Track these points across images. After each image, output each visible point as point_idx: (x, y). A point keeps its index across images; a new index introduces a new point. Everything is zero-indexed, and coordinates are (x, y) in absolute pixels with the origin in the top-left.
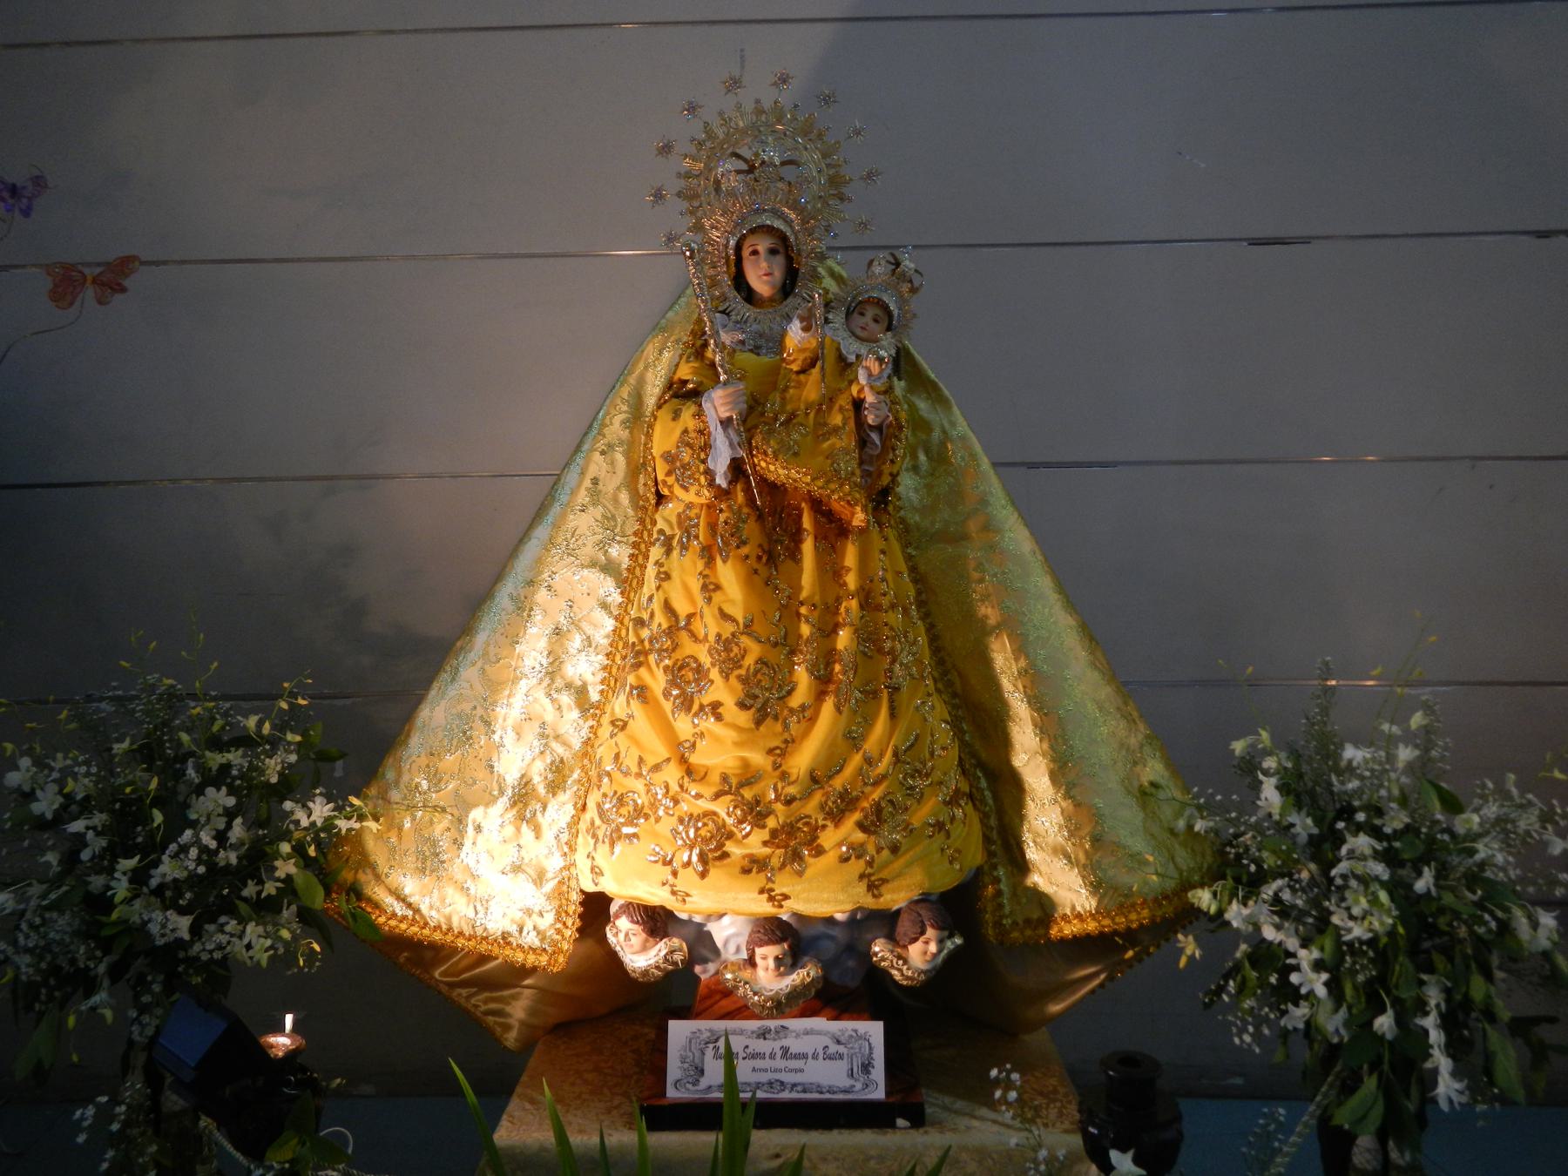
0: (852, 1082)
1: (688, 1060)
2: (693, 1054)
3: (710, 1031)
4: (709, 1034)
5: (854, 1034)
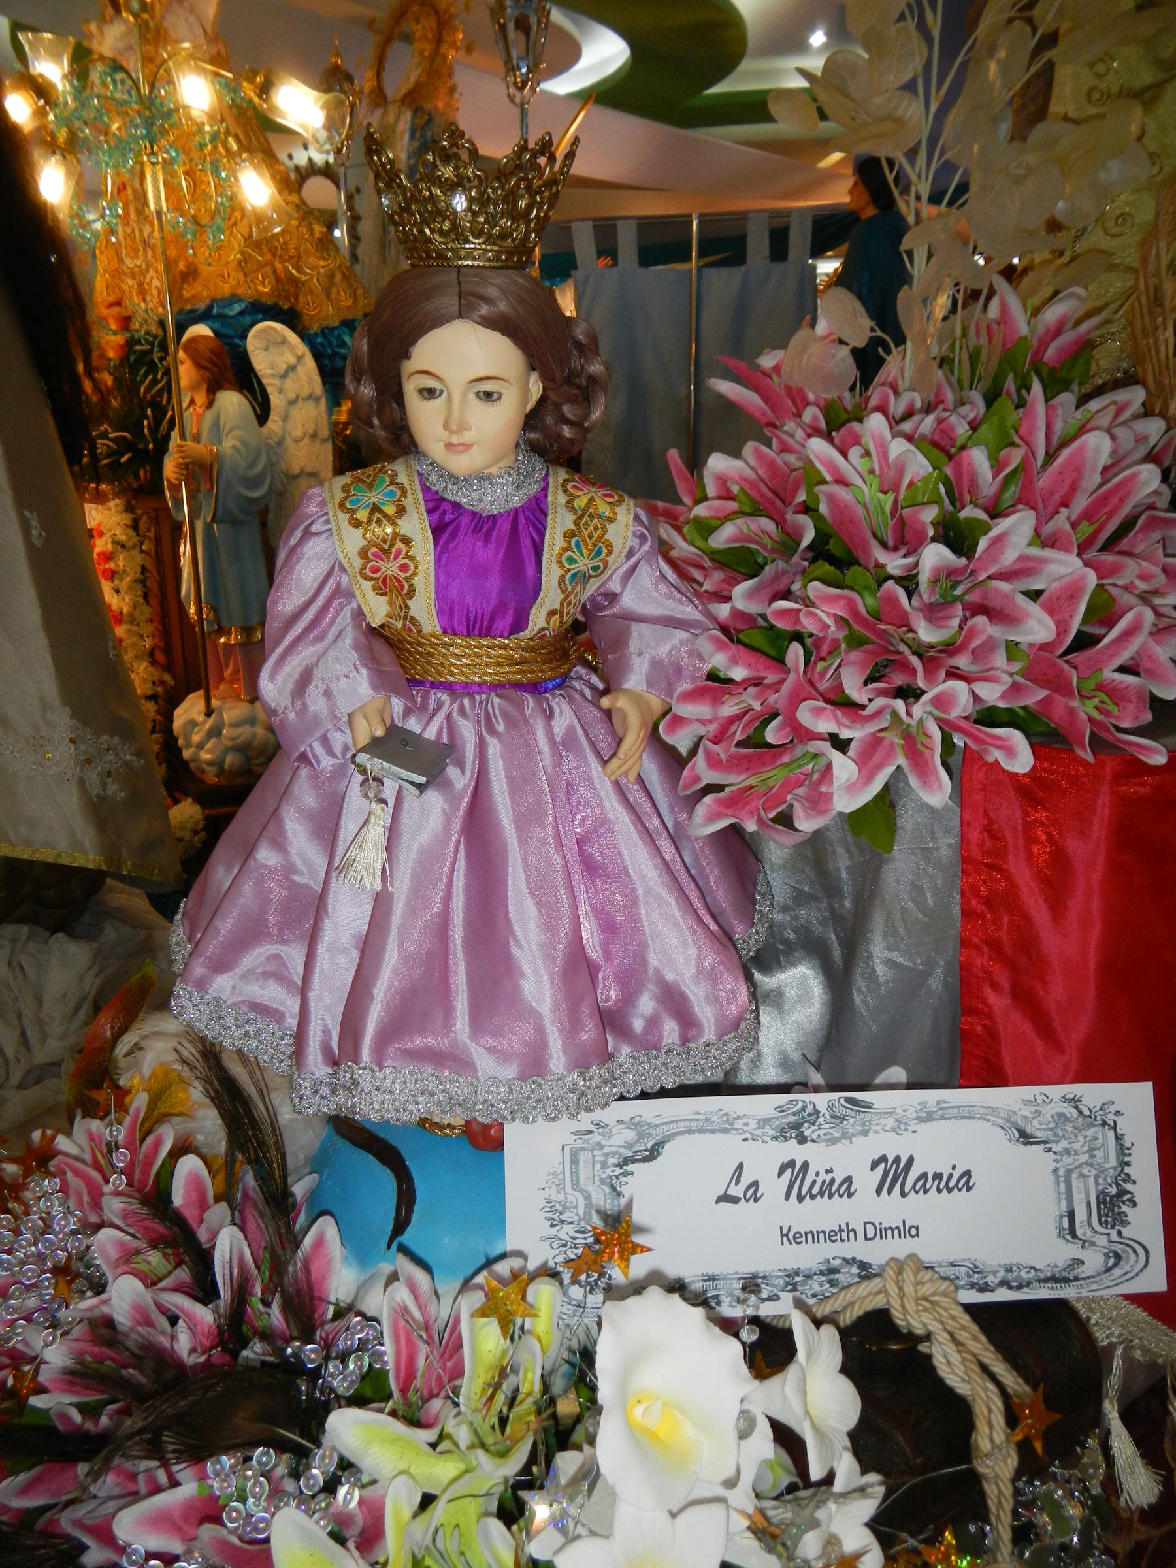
0: (1072, 1251)
1: (563, 1217)
3: (634, 1124)
4: (630, 1135)
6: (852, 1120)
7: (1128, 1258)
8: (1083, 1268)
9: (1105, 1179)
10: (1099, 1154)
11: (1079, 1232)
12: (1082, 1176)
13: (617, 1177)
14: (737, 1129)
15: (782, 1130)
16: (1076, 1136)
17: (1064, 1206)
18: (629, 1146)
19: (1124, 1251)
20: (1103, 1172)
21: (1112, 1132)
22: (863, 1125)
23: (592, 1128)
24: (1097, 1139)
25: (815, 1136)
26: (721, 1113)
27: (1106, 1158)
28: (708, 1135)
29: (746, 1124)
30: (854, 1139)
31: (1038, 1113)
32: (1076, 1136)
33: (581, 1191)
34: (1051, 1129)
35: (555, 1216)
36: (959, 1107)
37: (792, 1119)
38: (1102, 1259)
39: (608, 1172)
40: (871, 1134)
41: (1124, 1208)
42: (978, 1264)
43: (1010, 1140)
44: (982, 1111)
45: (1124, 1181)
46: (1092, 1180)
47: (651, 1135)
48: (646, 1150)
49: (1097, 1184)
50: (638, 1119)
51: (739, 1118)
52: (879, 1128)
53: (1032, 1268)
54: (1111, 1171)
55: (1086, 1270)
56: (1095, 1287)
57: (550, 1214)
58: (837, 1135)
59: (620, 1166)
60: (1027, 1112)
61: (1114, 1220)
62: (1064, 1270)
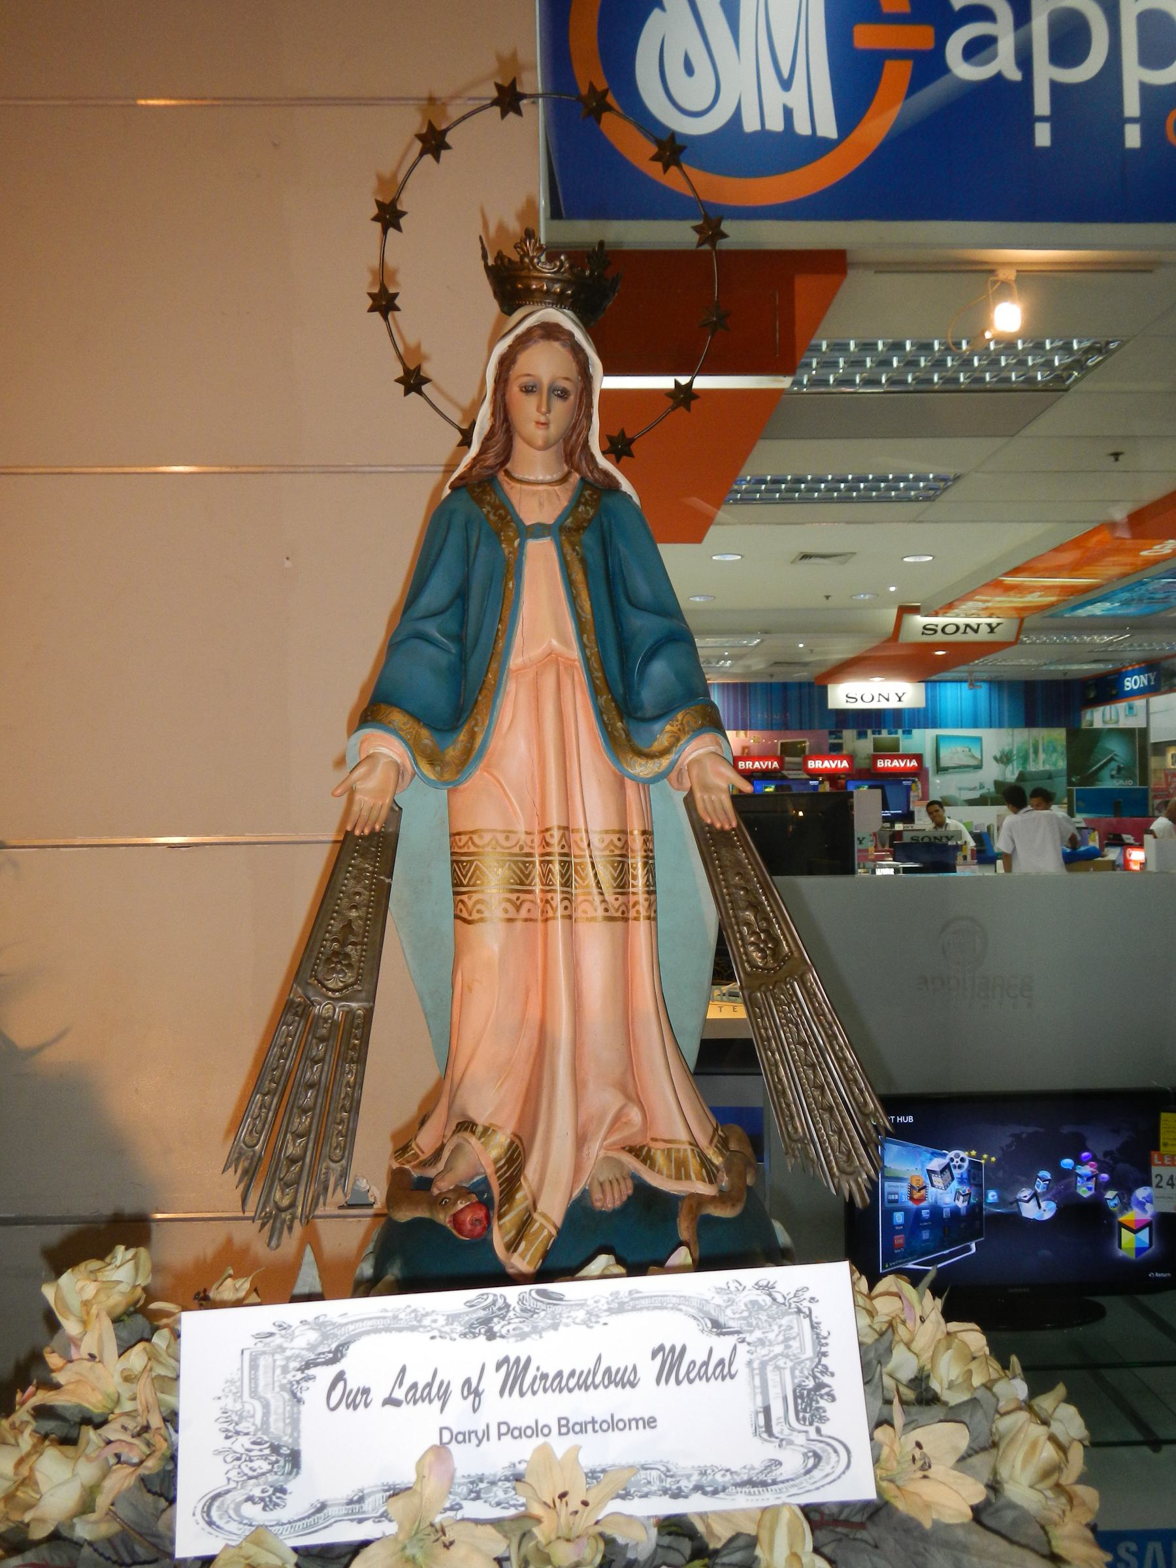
0: (770, 1450)
1: (239, 1428)
2: (266, 1406)
3: (318, 1324)
4: (313, 1336)
5: (764, 1299)
6: (543, 1314)
7: (829, 1458)
8: (781, 1470)
9: (801, 1372)
10: (795, 1344)
11: (776, 1429)
12: (778, 1368)
13: (298, 1382)
14: (425, 1327)
15: (471, 1326)
16: (770, 1325)
17: (759, 1402)
18: (312, 1348)
19: (824, 1451)
20: (800, 1363)
21: (808, 1319)
22: (554, 1318)
23: (274, 1330)
24: (791, 1328)
25: (504, 1331)
26: (409, 1310)
27: (802, 1348)
28: (395, 1334)
29: (435, 1321)
30: (544, 1334)
31: (731, 1302)
32: (770, 1325)
33: (259, 1399)
34: (744, 1318)
35: (231, 1428)
36: (651, 1297)
37: (482, 1314)
38: (800, 1459)
39: (289, 1377)
40: (561, 1328)
41: (822, 1403)
42: (671, 1467)
43: (702, 1331)
44: (674, 1300)
45: (822, 1373)
46: (787, 1373)
47: (335, 1336)
48: (329, 1352)
49: (793, 1377)
50: (321, 1319)
51: (427, 1314)
52: (570, 1320)
53: (727, 1470)
54: (808, 1363)
55: (783, 1472)
56: (794, 1491)
57: (225, 1425)
58: (527, 1329)
59: (301, 1370)
60: (719, 1300)
61: (812, 1416)
62: (761, 1472)
